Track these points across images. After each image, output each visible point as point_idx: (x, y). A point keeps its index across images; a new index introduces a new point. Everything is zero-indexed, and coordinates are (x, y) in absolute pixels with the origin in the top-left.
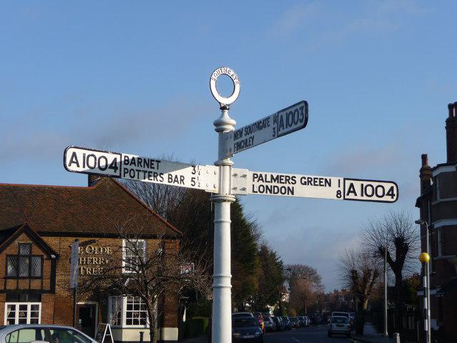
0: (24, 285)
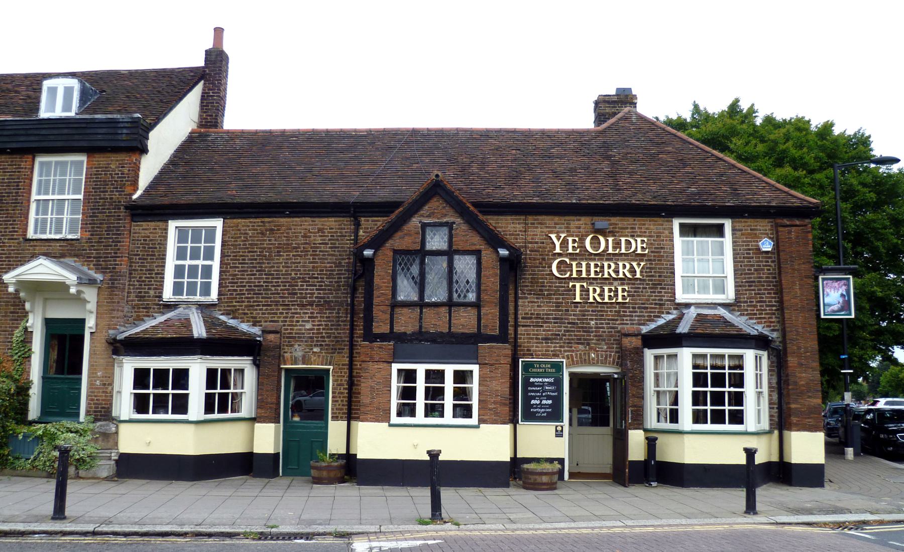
0: (435, 322)
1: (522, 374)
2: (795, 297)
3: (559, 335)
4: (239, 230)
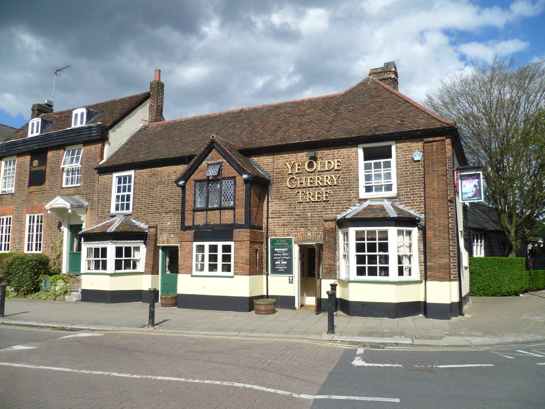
0: (214, 218)
1: (271, 247)
2: (434, 190)
3: (290, 222)
4: (141, 175)
